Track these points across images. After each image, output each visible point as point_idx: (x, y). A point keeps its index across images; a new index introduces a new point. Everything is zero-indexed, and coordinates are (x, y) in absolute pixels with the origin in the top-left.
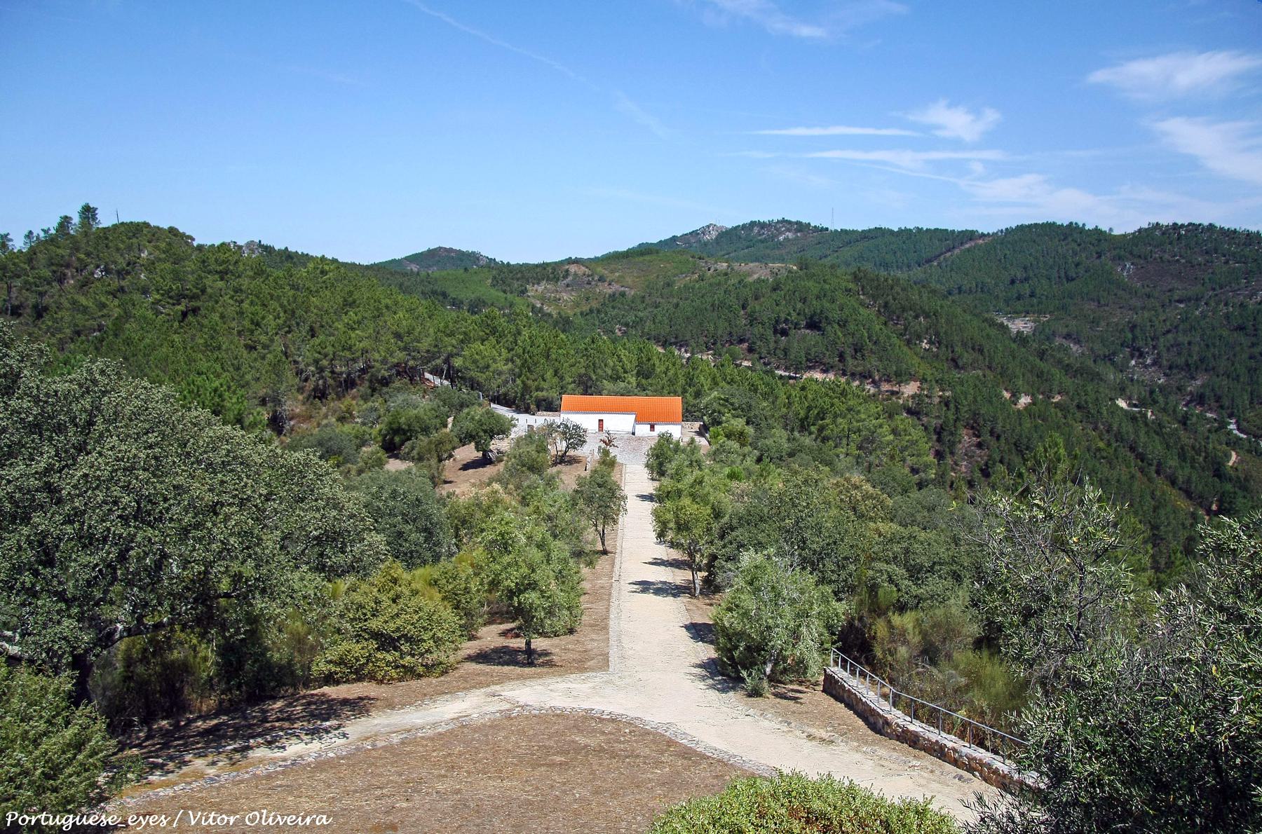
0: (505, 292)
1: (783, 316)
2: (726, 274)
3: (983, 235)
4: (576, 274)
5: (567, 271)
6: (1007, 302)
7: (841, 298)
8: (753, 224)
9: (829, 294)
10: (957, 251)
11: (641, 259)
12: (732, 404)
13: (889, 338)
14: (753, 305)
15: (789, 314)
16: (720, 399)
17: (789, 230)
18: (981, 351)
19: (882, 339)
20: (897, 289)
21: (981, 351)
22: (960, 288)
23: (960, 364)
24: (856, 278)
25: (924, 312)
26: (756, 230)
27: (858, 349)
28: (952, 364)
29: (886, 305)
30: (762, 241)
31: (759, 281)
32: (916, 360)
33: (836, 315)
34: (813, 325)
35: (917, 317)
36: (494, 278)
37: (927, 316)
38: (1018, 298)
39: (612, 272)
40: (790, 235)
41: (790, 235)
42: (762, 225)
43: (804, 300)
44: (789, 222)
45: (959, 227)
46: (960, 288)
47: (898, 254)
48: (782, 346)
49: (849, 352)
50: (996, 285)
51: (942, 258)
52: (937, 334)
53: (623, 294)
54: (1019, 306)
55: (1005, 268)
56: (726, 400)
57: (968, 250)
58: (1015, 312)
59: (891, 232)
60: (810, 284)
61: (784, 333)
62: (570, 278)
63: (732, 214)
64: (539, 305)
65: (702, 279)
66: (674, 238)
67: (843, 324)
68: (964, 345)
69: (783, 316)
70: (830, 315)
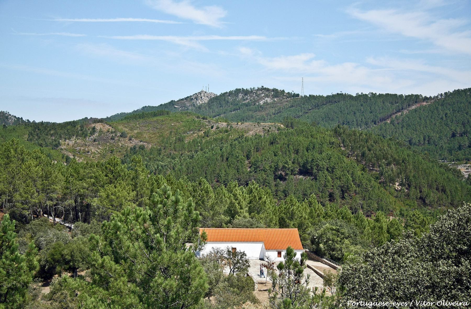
0: (41, 145)
1: (281, 165)
2: (227, 131)
3: (426, 99)
4: (101, 131)
5: (94, 128)
6: (450, 151)
7: (328, 151)
8: (238, 91)
9: (317, 146)
10: (405, 112)
11: (155, 119)
12: (343, 234)
13: (370, 181)
14: (255, 156)
15: (286, 163)
16: (332, 230)
17: (267, 96)
18: (444, 191)
19: (364, 181)
20: (371, 142)
21: (444, 191)
22: (410, 142)
23: (427, 202)
24: (336, 133)
25: (395, 160)
26: (240, 96)
27: (344, 191)
28: (420, 202)
29: (363, 155)
30: (246, 105)
31: (257, 137)
32: (392, 199)
33: (324, 164)
34: (305, 171)
35: (388, 164)
36: (31, 134)
37: (397, 163)
38: (460, 148)
39: (132, 129)
40: (269, 100)
41: (269, 100)
42: (246, 92)
43: (297, 152)
44: (268, 90)
45: (406, 92)
46: (410, 142)
47: (358, 114)
48: (281, 188)
49: (337, 193)
50: (440, 138)
51: (394, 116)
52: (407, 178)
53: (142, 148)
54: (460, 154)
55: (447, 125)
56: (338, 231)
57: (416, 110)
58: (458, 160)
59: (351, 97)
60: (301, 138)
61: (282, 178)
62: (97, 134)
63: (220, 84)
64: (72, 157)
65: (207, 134)
66: (172, 103)
67: (331, 170)
68: (430, 187)
69: (281, 165)
70: (320, 163)
